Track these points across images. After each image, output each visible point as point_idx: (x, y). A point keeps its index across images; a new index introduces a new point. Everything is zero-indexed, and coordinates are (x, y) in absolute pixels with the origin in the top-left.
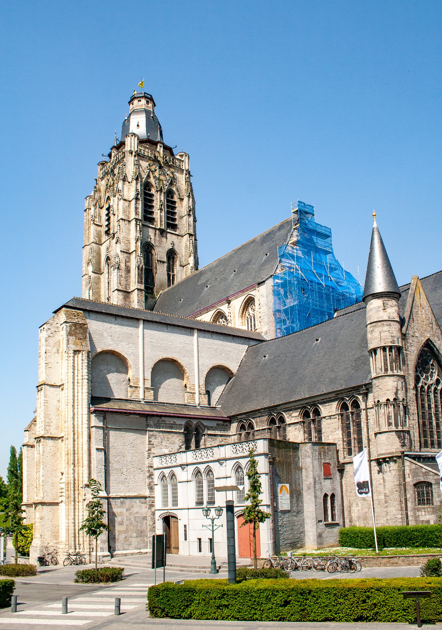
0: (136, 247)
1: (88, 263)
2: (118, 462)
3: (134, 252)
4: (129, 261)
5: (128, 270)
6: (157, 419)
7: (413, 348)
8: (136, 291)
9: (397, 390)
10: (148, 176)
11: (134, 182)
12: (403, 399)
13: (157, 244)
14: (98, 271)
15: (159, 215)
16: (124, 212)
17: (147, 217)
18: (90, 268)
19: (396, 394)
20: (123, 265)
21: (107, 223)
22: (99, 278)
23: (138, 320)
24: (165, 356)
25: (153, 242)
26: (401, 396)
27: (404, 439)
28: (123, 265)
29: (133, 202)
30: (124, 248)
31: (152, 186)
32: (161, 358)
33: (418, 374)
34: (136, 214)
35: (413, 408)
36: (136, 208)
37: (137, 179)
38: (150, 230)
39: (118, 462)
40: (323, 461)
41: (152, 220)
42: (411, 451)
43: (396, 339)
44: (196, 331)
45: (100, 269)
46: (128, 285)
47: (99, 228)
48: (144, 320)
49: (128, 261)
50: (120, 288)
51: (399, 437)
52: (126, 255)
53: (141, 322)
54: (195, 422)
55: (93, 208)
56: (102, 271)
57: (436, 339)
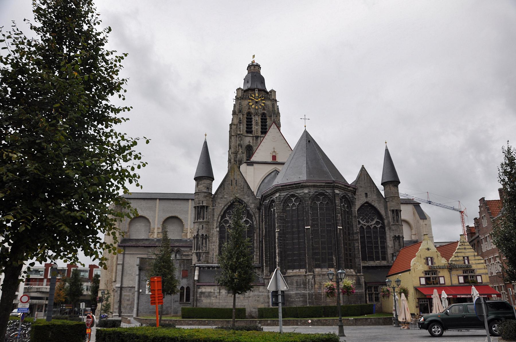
2: (130, 270)
6: (153, 249)
7: (220, 205)
9: (198, 230)
10: (249, 109)
12: (203, 235)
13: (254, 144)
17: (249, 130)
19: (198, 232)
23: (156, 199)
24: (171, 215)
25: (251, 144)
26: (200, 234)
27: (200, 257)
31: (252, 113)
32: (168, 216)
33: (228, 218)
35: (215, 239)
38: (249, 138)
39: (130, 270)
40: (182, 269)
41: (251, 132)
42: (208, 263)
43: (201, 202)
44: (190, 201)
48: (160, 199)
51: (197, 256)
53: (158, 200)
54: (176, 249)
57: (246, 197)
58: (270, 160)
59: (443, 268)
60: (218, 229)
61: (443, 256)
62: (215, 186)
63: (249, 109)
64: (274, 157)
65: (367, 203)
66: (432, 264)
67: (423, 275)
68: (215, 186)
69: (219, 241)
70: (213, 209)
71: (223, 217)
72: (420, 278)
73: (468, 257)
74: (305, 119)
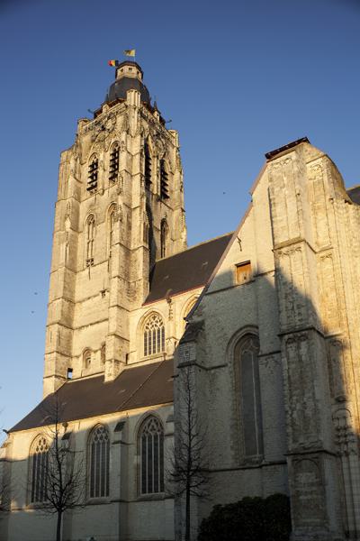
0: (141, 203)
1: (66, 218)
3: (138, 209)
4: (131, 218)
5: (129, 227)
8: (142, 249)
11: (139, 137)
14: (75, 228)
15: (155, 179)
16: (127, 165)
18: (68, 224)
20: (125, 219)
21: (90, 180)
22: (77, 238)
28: (125, 219)
29: (138, 157)
30: (126, 201)
34: (141, 170)
36: (141, 165)
37: (142, 136)
45: (78, 228)
46: (129, 242)
47: (79, 185)
49: (129, 217)
50: (122, 243)
52: (128, 210)
55: (72, 162)
56: (80, 230)
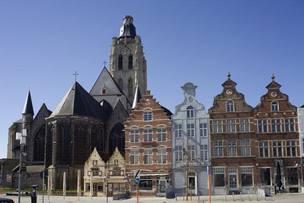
58: (101, 93)
59: (102, 166)
60: (33, 143)
61: (103, 159)
62: (34, 117)
63: (121, 52)
64: (104, 91)
65: (119, 123)
66: (96, 164)
67: (90, 170)
68: (34, 117)
69: (34, 148)
70: (31, 132)
71: (36, 136)
72: (88, 172)
73: (117, 160)
74: (76, 74)
